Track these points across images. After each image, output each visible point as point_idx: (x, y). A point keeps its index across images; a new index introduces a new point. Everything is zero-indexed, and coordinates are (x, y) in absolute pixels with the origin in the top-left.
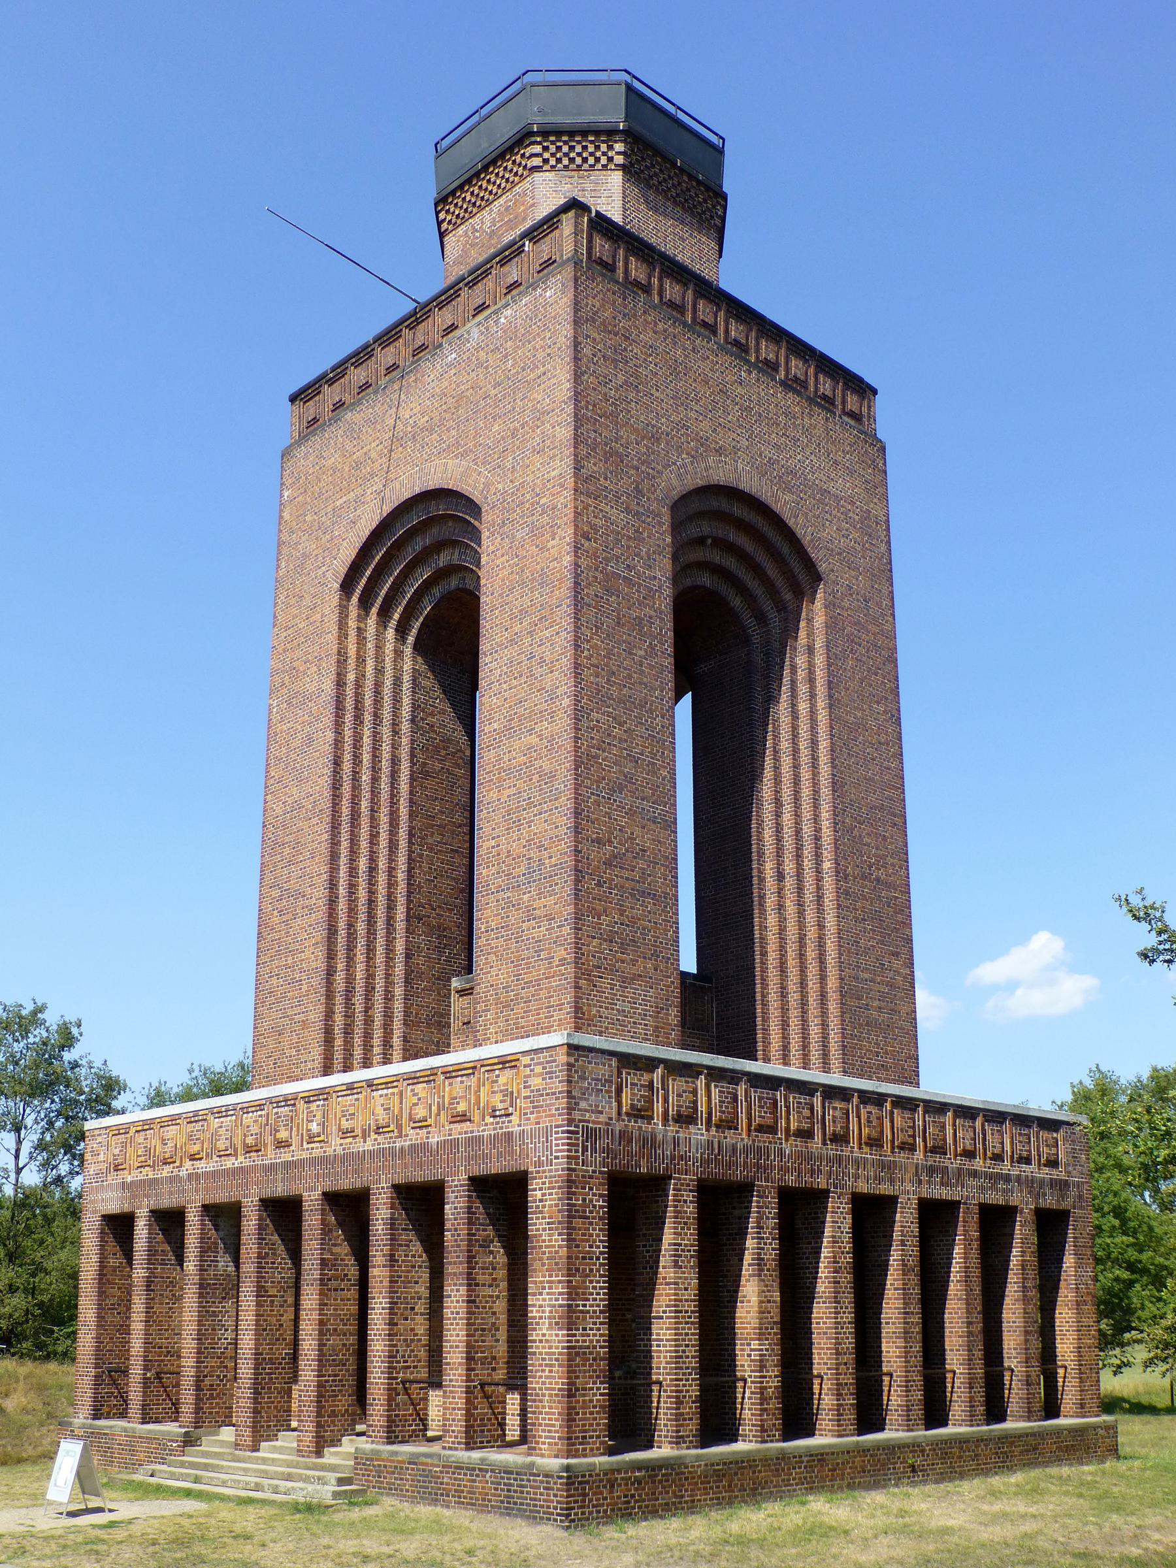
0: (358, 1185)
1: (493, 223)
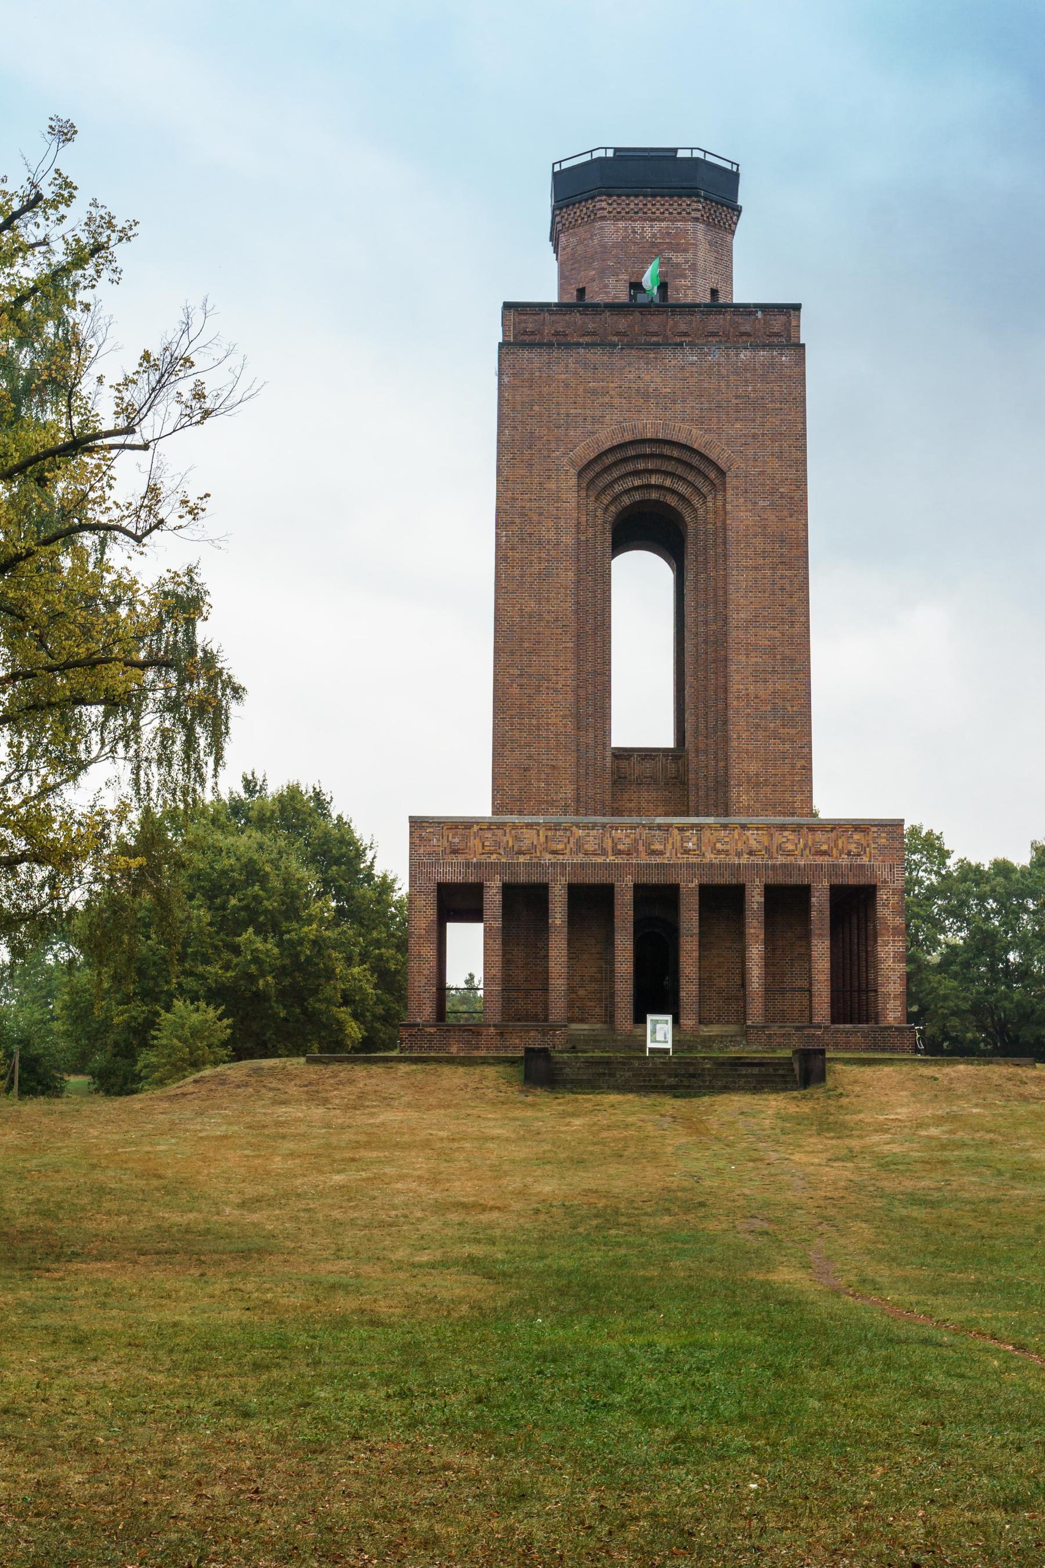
0: (734, 882)
1: (654, 235)
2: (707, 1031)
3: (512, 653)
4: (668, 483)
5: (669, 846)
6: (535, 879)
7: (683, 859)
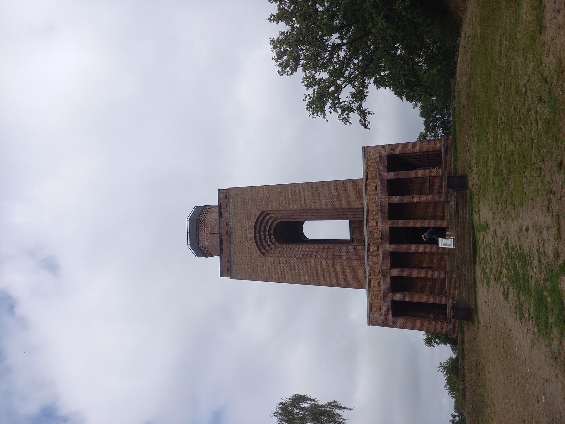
0: (387, 207)
2: (447, 217)
3: (317, 279)
4: (268, 228)
5: (375, 231)
6: (389, 281)
7: (380, 227)
